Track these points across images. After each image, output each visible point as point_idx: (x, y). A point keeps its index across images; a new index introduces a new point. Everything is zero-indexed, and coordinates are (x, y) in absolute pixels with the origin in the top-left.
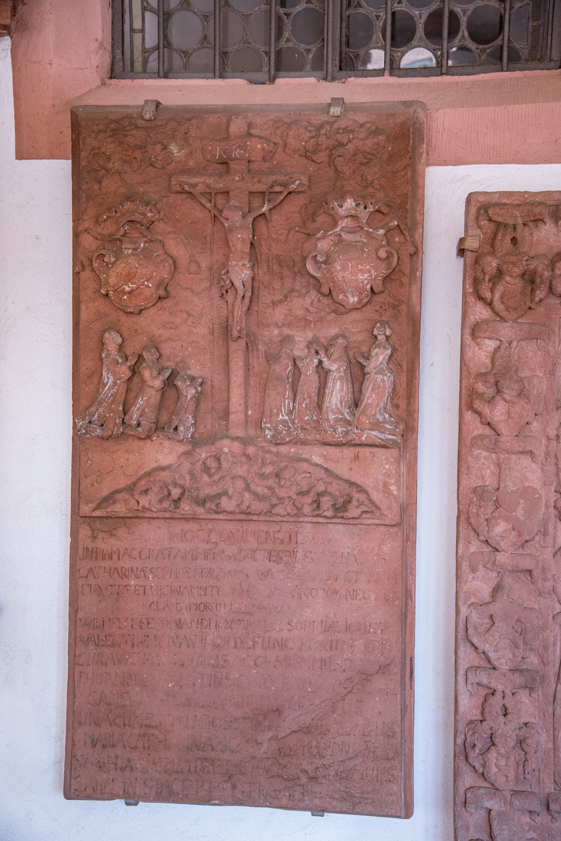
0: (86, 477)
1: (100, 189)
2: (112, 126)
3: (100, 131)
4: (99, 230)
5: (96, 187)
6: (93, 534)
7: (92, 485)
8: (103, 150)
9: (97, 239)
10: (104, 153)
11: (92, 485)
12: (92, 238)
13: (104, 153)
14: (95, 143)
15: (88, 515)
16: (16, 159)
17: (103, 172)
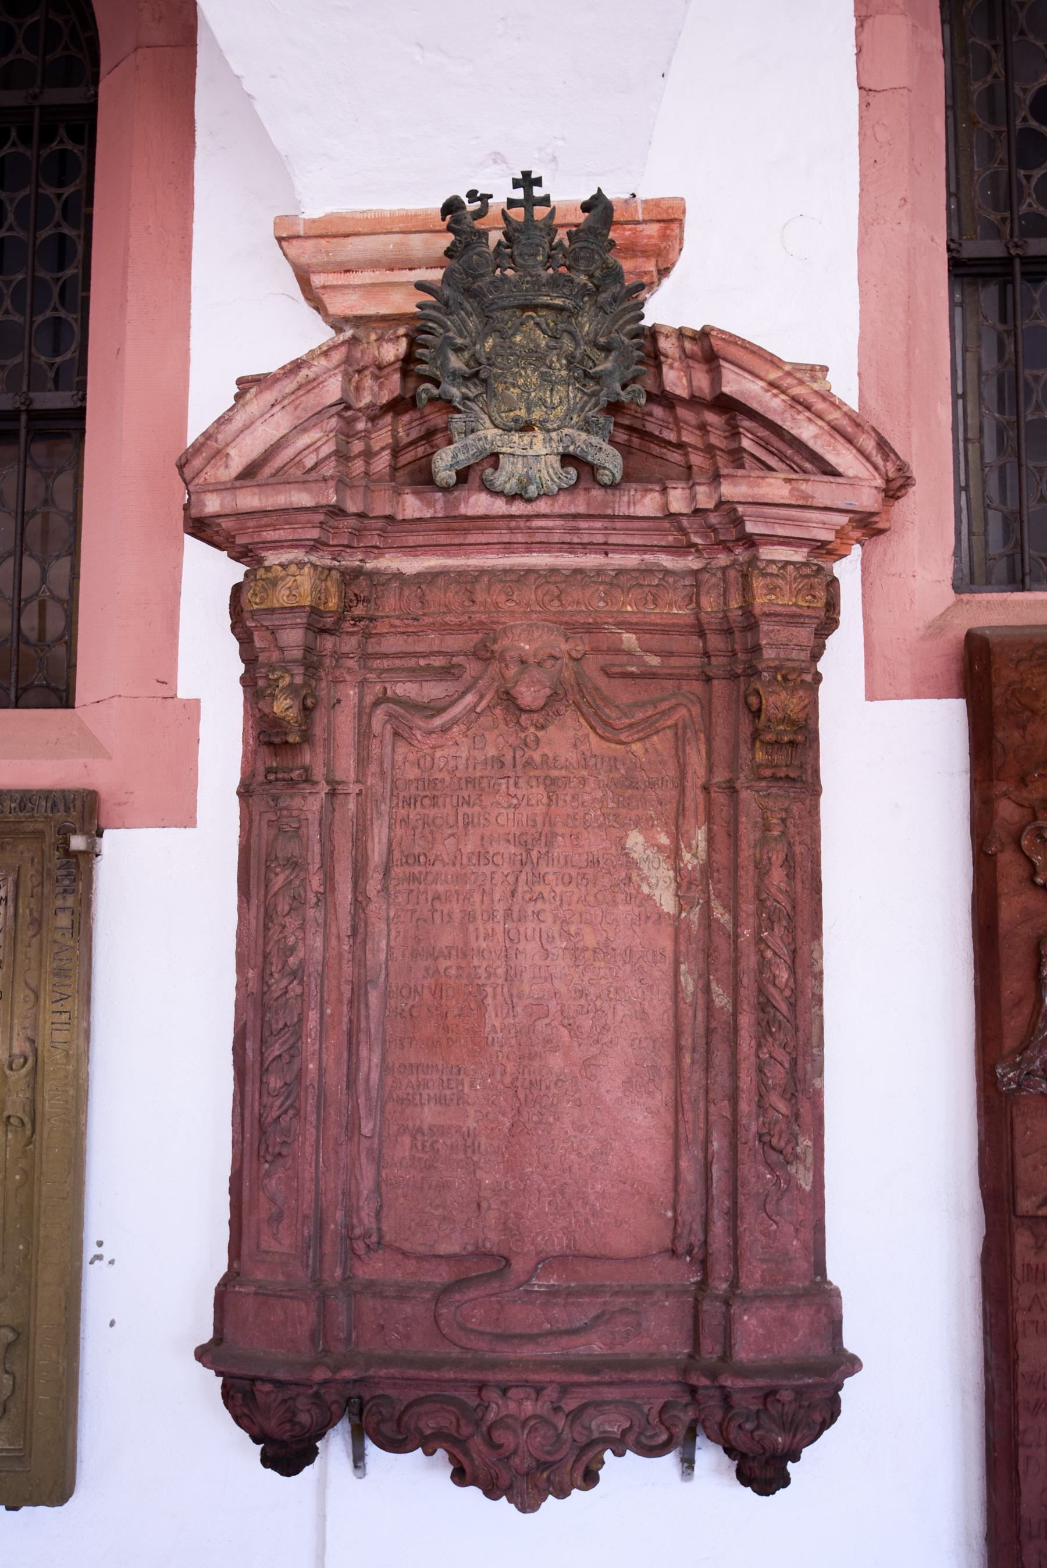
0: (1025, 1156)
1: (1023, 737)
2: (1040, 652)
3: (1020, 661)
4: (1025, 793)
5: (1016, 735)
6: (1036, 1243)
7: (1035, 1168)
8: (1028, 684)
9: (1022, 806)
10: (1029, 689)
11: (1035, 1168)
12: (1013, 805)
13: (1029, 689)
14: (1014, 676)
15: (1031, 1213)
16: (867, 699)
17: (1028, 713)
